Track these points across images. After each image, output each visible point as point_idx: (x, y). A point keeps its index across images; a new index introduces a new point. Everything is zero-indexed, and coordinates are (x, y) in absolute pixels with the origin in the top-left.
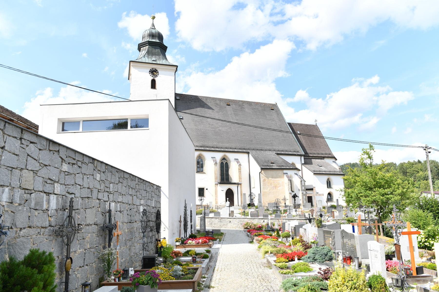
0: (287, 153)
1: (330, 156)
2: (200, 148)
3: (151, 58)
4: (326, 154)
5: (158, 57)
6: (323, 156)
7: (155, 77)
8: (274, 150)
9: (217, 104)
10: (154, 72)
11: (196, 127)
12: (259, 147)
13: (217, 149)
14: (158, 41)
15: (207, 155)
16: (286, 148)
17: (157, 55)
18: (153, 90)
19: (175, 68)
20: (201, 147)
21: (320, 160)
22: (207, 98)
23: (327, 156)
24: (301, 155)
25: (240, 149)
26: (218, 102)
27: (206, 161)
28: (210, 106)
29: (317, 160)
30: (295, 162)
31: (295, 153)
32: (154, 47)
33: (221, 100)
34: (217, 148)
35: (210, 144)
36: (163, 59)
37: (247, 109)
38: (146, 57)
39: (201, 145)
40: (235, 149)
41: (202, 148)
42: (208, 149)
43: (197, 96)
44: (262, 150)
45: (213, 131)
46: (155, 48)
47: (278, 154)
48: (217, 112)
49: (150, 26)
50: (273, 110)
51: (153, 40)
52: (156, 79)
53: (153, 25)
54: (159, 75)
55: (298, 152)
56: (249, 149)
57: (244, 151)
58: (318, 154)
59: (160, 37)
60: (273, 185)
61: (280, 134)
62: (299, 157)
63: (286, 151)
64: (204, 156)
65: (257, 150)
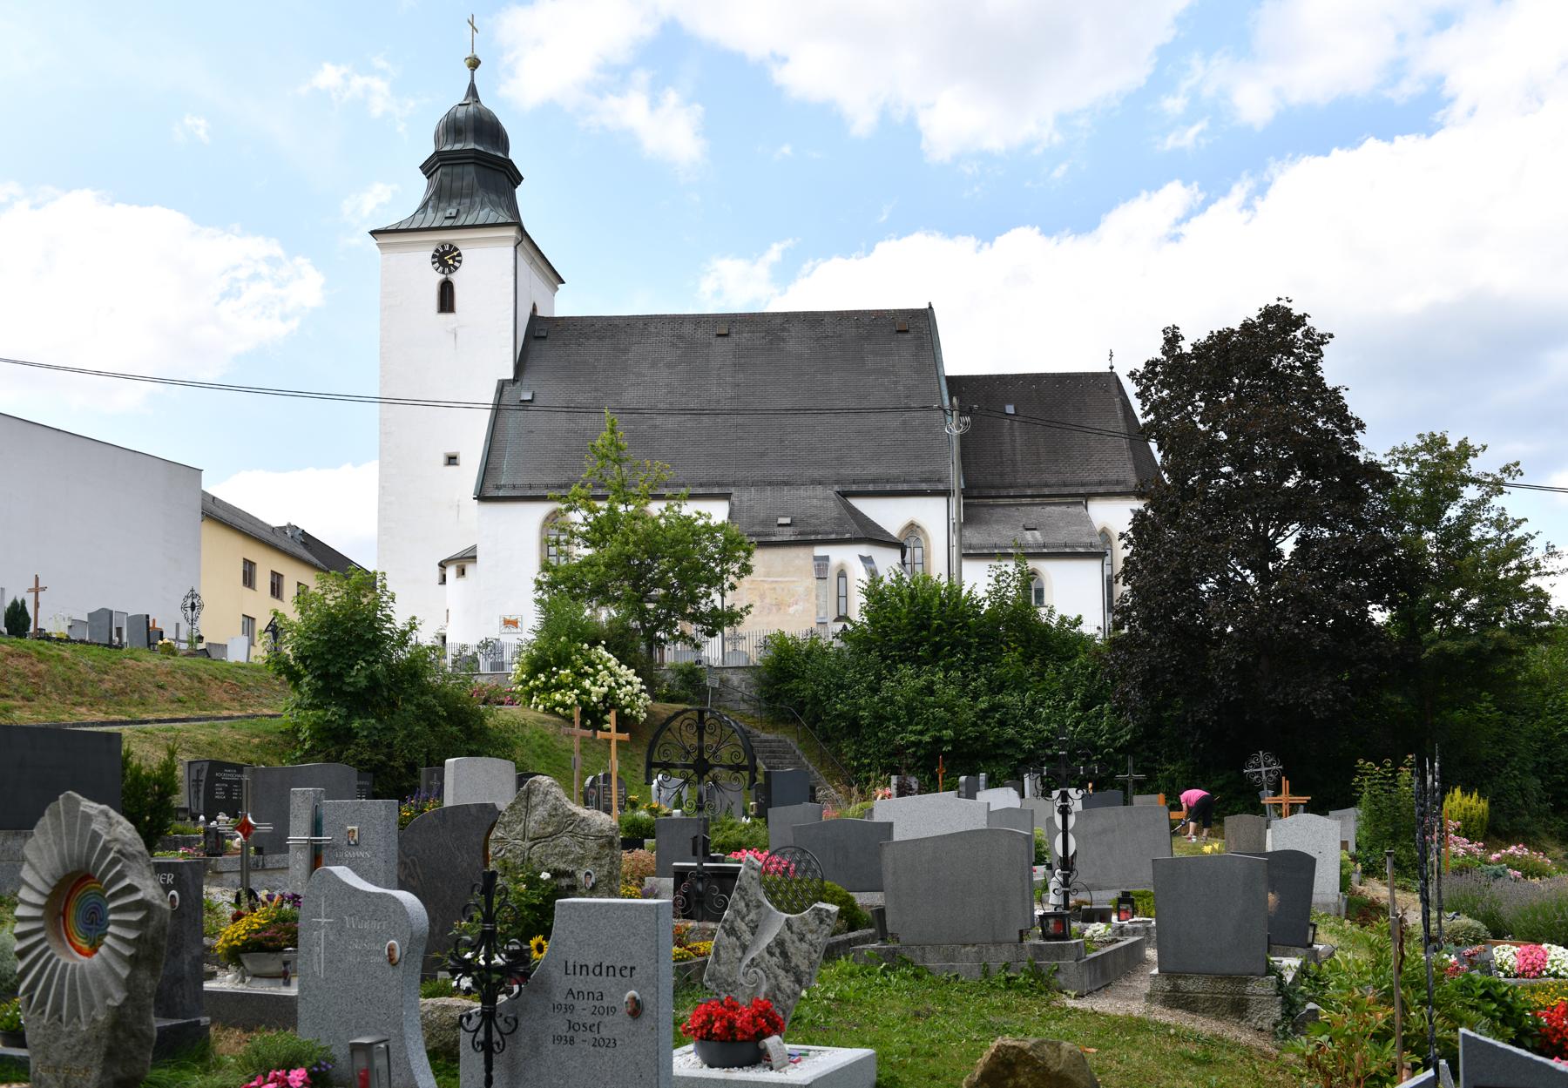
1: (1118, 489)
4: (1100, 483)
5: (467, 201)
6: (1082, 491)
8: (837, 482)
9: (680, 337)
10: (446, 258)
12: (780, 473)
14: (471, 146)
16: (895, 472)
17: (467, 196)
18: (446, 317)
19: (512, 232)
21: (1064, 508)
23: (1101, 490)
25: (701, 485)
26: (687, 329)
29: (1048, 509)
30: (920, 521)
31: (924, 486)
36: (482, 208)
40: (683, 486)
44: (786, 484)
49: (460, 96)
50: (906, 331)
52: (455, 278)
53: (472, 91)
55: (939, 481)
56: (734, 484)
57: (716, 490)
60: (768, 600)
61: (893, 421)
62: (942, 501)
63: (888, 481)
65: (770, 484)
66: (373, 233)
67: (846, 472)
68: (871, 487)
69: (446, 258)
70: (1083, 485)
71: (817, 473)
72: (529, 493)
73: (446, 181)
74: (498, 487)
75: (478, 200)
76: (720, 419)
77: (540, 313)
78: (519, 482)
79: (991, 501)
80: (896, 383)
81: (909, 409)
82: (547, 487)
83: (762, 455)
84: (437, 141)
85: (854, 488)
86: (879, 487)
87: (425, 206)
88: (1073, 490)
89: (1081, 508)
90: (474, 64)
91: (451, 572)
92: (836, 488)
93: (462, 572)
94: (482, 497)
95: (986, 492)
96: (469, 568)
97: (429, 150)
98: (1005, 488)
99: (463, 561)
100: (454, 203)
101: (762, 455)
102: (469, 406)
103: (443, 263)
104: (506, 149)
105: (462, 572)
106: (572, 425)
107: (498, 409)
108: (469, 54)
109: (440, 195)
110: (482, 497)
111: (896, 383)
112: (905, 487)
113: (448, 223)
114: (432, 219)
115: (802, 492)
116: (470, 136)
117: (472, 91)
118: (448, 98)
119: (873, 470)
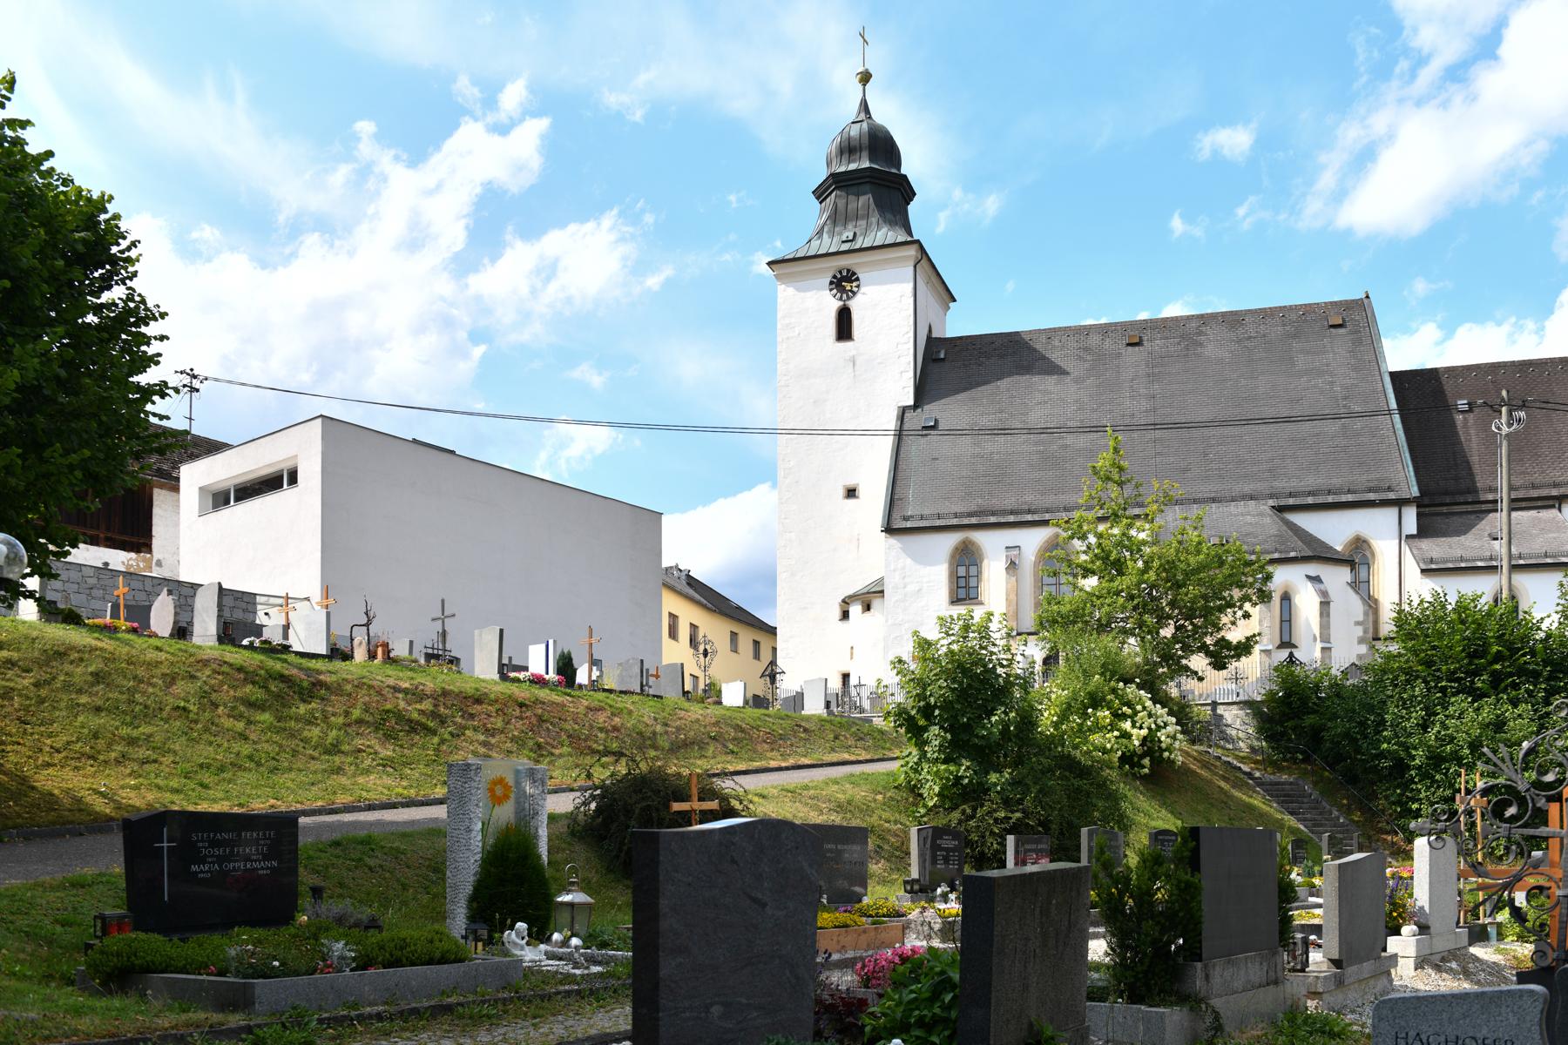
0: (1330, 499)
2: (966, 521)
3: (840, 234)
5: (863, 223)
6: (1555, 492)
7: (849, 298)
8: (1271, 496)
10: (844, 282)
11: (978, 450)
12: (1206, 489)
13: (1029, 518)
14: (866, 164)
15: (993, 545)
16: (1336, 482)
19: (912, 252)
20: (970, 515)
21: (1533, 513)
22: (1051, 333)
24: (1400, 503)
27: (985, 563)
28: (1059, 362)
30: (1366, 533)
31: (1372, 496)
32: (854, 189)
33: (1105, 330)
34: (1029, 512)
35: (1010, 502)
36: (879, 229)
37: (1214, 347)
38: (825, 236)
39: (973, 508)
41: (974, 520)
42: (993, 519)
43: (1017, 333)
44: (1214, 500)
45: (1039, 452)
46: (858, 195)
47: (1280, 509)
48: (1077, 381)
49: (852, 110)
51: (853, 166)
52: (856, 305)
53: (865, 107)
54: (863, 289)
55: (1390, 489)
58: (1534, 487)
59: (881, 145)
61: (1332, 427)
62: (1392, 513)
63: (1329, 492)
64: (979, 549)
65: (1195, 501)
66: (769, 264)
67: (1281, 484)
68: (1310, 500)
69: (844, 282)
70: (1556, 485)
71: (1248, 488)
72: (938, 523)
73: (841, 203)
74: (906, 519)
75: (874, 220)
76: (1135, 435)
77: (934, 335)
78: (926, 512)
79: (1445, 509)
80: (1332, 383)
81: (1351, 415)
82: (956, 515)
83: (1185, 470)
84: (829, 164)
85: (1291, 501)
86: (1320, 500)
87: (820, 233)
88: (1544, 492)
89: (1554, 512)
90: (865, 78)
91: (855, 610)
92: (1271, 502)
93: (868, 608)
94: (889, 530)
95: (1438, 500)
96: (876, 604)
97: (821, 174)
98: (1462, 493)
99: (868, 598)
100: (850, 226)
101: (1185, 470)
102: (865, 432)
103: (841, 289)
104: (898, 166)
105: (868, 608)
106: (978, 450)
107: (900, 435)
108: (861, 69)
109: (837, 219)
110: (889, 530)
111: (1332, 383)
112: (1350, 498)
113: (845, 247)
114: (828, 244)
115: (1233, 508)
116: (865, 154)
117: (865, 107)
118: (841, 116)
119: (1311, 481)
